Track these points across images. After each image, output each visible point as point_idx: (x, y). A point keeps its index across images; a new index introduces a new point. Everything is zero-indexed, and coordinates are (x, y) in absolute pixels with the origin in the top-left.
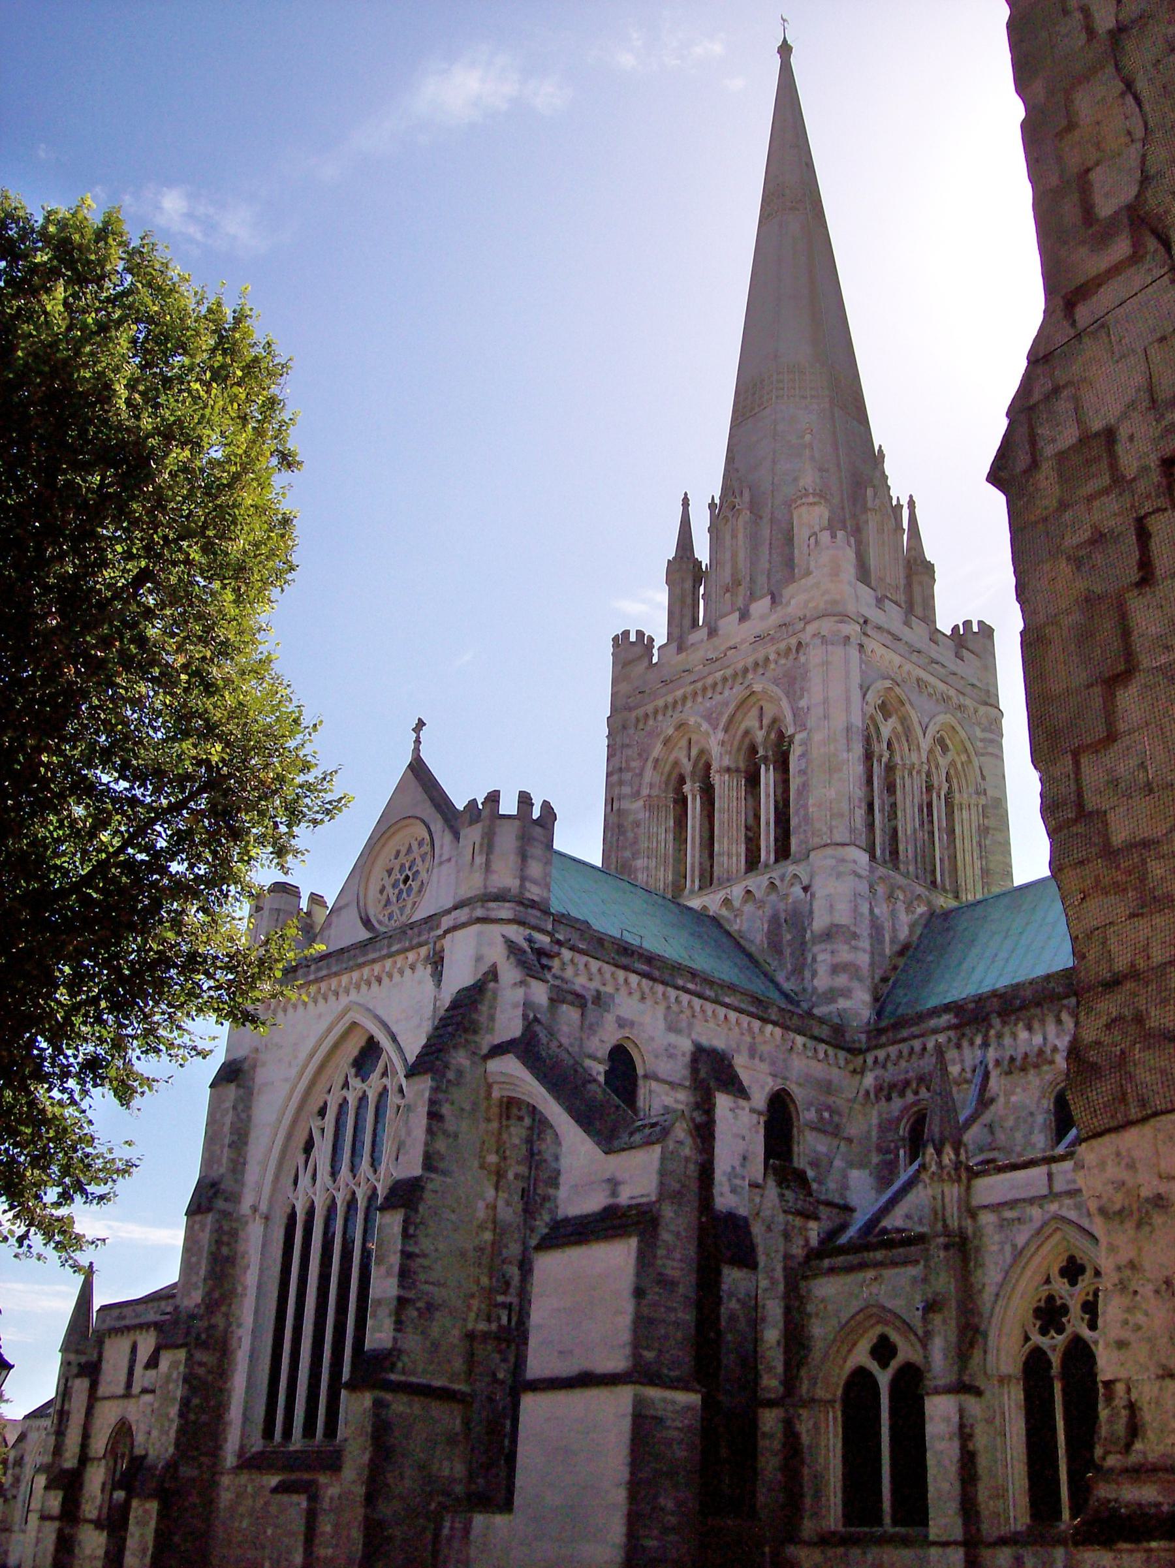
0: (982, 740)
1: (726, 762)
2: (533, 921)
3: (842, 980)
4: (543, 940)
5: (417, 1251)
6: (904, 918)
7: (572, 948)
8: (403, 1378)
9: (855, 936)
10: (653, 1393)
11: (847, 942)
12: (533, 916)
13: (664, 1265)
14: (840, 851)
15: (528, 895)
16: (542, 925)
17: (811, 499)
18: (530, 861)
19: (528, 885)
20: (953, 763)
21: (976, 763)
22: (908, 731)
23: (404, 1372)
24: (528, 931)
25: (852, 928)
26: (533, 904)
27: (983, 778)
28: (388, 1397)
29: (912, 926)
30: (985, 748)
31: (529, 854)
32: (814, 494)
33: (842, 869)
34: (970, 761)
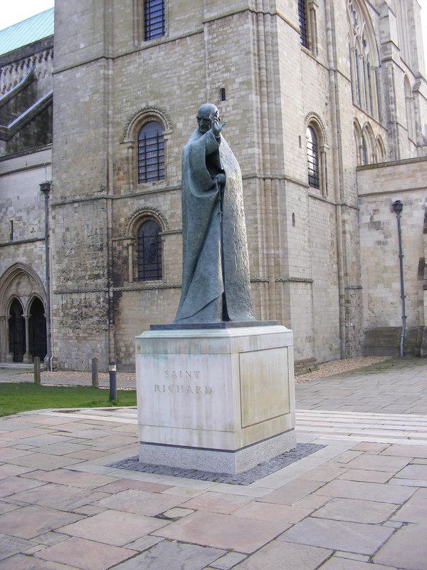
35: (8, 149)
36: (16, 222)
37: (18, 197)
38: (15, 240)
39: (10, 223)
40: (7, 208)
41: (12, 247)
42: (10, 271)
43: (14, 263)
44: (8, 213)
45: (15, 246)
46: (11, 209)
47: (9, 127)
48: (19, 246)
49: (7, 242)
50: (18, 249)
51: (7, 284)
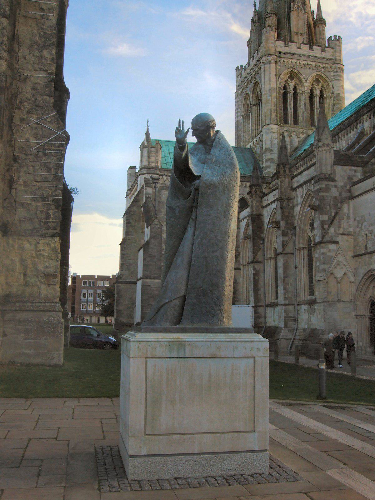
0: (333, 76)
1: (254, 103)
2: (152, 172)
3: (268, 164)
4: (156, 176)
5: (125, 253)
6: (296, 140)
7: (166, 176)
8: (124, 280)
9: (271, 150)
10: (148, 281)
11: (270, 152)
12: (152, 171)
13: (151, 253)
14: (268, 127)
15: (151, 166)
16: (155, 172)
17: (269, 15)
18: (151, 157)
19: (150, 163)
20: (322, 86)
21: (330, 84)
22: (301, 81)
23: (124, 279)
24: (151, 175)
25: (271, 148)
26: (153, 168)
27: (333, 88)
28: (120, 285)
29: (299, 142)
30: (334, 78)
31: (150, 156)
32: (270, 14)
33: (268, 132)
34: (328, 84)
35: (364, 173)
36: (369, 235)
37: (369, 213)
38: (369, 250)
39: (365, 236)
40: (362, 224)
41: (367, 256)
42: (366, 277)
43: (369, 270)
44: (363, 228)
45: (369, 255)
46: (365, 224)
47: (366, 155)
48: (372, 254)
49: (363, 252)
50: (371, 258)
51: (365, 288)
